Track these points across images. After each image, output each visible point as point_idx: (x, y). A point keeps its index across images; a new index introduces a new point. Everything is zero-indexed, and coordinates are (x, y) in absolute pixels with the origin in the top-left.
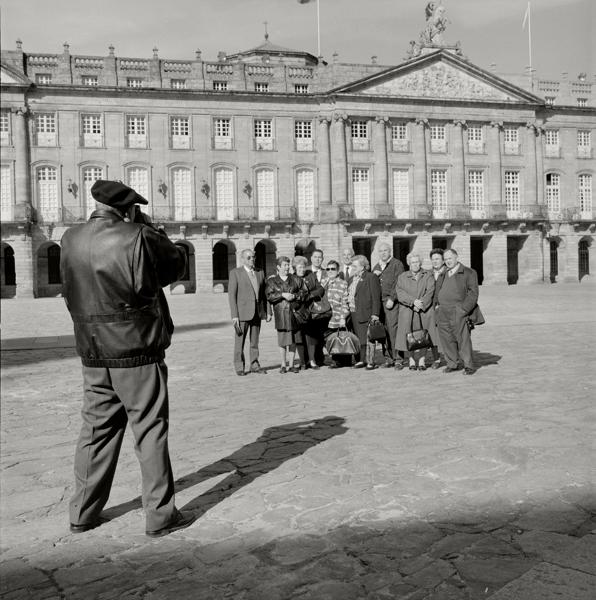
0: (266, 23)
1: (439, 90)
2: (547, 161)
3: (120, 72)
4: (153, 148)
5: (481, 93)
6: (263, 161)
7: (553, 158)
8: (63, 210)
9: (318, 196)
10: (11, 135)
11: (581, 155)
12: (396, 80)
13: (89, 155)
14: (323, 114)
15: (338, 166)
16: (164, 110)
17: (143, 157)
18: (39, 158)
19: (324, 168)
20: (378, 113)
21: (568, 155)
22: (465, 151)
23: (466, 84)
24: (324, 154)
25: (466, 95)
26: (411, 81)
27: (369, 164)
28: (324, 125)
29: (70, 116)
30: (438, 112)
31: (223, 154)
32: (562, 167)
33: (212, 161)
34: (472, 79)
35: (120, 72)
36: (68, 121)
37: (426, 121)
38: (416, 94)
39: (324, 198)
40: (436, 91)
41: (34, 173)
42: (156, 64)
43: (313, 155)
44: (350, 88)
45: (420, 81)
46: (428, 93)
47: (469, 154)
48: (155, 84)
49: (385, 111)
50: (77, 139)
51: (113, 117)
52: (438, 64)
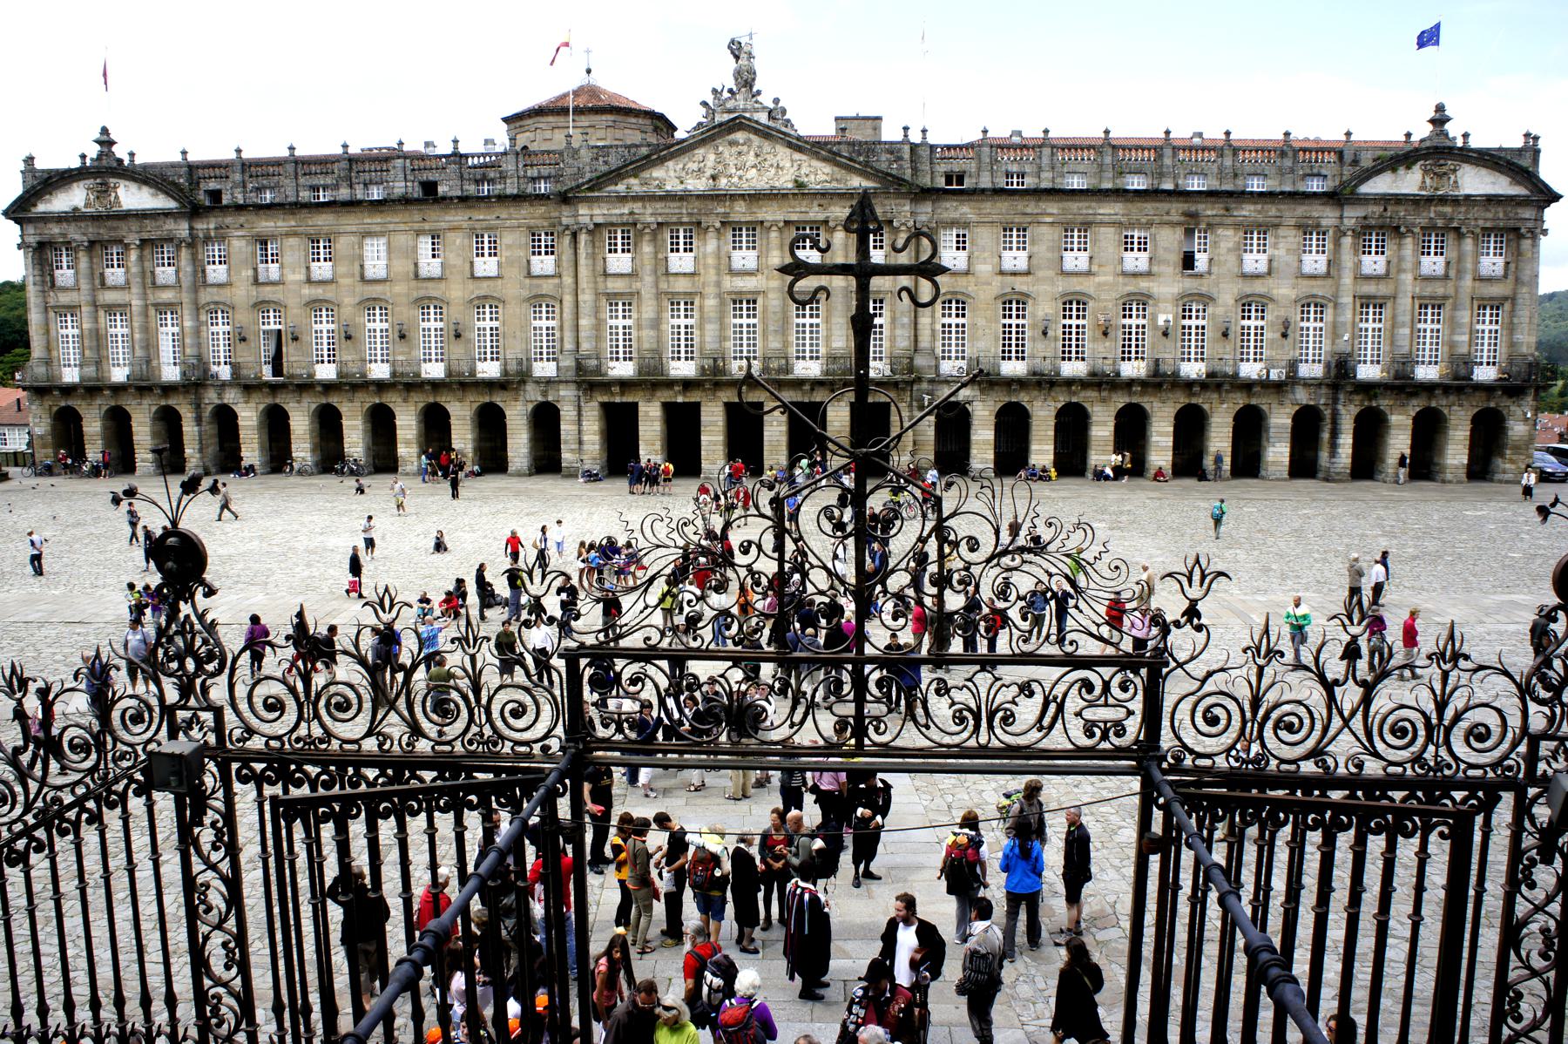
0: (588, 52)
1: (740, 178)
3: (302, 180)
4: (342, 281)
5: (812, 177)
6: (482, 293)
8: (236, 368)
10: (177, 272)
11: (1008, 265)
12: (670, 164)
13: (268, 293)
14: (565, 221)
16: (354, 229)
18: (208, 299)
19: (568, 299)
20: (642, 218)
21: (984, 268)
23: (788, 165)
24: (568, 280)
25: (785, 181)
26: (695, 166)
27: (631, 294)
28: (567, 240)
29: (243, 243)
30: (740, 211)
31: (430, 285)
32: (971, 289)
33: (415, 295)
34: (797, 156)
35: (302, 180)
36: (239, 245)
37: (718, 225)
38: (698, 185)
40: (735, 180)
42: (344, 164)
43: (556, 281)
44: (597, 183)
46: (723, 182)
48: (344, 193)
49: (648, 214)
50: (250, 273)
51: (292, 241)
52: (740, 136)
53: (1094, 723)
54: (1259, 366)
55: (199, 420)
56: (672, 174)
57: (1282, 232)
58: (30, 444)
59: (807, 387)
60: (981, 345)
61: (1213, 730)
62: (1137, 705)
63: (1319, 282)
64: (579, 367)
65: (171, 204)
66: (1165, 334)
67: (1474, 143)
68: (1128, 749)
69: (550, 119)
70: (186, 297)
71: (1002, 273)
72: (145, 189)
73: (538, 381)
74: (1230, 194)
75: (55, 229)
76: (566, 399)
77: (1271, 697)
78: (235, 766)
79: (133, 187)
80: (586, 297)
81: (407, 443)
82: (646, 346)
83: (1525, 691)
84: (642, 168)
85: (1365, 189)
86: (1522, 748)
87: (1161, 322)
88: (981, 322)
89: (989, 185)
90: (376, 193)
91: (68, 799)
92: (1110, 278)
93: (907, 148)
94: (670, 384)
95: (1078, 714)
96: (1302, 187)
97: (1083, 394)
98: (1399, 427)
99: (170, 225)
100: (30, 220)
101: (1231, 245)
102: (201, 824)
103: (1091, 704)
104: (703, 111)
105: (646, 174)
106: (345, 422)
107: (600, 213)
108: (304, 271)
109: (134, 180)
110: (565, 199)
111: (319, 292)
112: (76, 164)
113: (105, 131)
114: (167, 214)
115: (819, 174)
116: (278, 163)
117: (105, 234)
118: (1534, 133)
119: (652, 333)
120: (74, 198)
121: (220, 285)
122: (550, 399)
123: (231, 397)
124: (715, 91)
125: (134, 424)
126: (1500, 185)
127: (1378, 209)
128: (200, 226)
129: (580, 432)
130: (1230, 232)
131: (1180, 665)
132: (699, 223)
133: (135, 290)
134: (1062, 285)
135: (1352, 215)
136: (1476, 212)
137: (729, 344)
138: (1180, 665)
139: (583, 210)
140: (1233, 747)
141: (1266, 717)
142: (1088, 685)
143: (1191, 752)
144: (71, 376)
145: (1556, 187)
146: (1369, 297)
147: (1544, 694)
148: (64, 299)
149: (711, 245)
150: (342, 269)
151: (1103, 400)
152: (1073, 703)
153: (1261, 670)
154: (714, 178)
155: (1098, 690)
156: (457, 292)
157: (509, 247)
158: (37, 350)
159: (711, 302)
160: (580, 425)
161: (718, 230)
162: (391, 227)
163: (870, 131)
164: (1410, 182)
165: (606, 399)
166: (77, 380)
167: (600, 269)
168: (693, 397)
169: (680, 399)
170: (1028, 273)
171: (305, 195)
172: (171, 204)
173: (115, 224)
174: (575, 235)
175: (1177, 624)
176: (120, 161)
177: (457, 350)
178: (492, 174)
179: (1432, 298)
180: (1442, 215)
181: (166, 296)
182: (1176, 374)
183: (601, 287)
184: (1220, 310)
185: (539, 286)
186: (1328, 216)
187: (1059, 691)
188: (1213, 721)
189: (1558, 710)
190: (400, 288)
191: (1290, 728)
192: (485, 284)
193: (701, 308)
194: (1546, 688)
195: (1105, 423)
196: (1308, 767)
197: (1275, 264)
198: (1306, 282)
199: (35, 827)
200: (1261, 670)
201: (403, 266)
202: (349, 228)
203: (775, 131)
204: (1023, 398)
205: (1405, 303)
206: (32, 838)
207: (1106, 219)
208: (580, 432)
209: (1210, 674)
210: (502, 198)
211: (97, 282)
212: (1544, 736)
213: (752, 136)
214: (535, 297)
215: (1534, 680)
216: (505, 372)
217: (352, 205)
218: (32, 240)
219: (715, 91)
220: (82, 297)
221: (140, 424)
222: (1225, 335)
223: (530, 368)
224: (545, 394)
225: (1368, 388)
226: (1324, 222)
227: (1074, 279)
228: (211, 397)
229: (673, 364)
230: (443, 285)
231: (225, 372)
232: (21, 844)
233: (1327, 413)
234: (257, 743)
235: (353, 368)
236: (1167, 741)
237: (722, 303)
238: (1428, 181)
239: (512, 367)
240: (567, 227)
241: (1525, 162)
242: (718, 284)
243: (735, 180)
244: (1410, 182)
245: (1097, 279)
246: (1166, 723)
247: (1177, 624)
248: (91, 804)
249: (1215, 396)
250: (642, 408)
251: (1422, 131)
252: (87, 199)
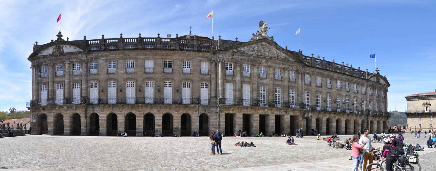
2: (306, 86)
7: (308, 85)
9: (210, 94)
12: (246, 47)
19: (213, 82)
24: (213, 76)
28: (213, 65)
39: (213, 95)
43: (209, 76)
60: (313, 103)
71: (317, 86)
73: (204, 106)
84: (238, 47)
88: (313, 98)
105: (239, 49)
122: (206, 113)
129: (219, 122)
134: (327, 91)
151: (335, 117)
157: (194, 66)
160: (219, 120)
165: (227, 112)
170: (321, 87)
174: (216, 64)
183: (225, 79)
195: (335, 122)
203: (272, 42)
208: (219, 122)
224: (205, 110)
240: (214, 61)
243: (263, 54)
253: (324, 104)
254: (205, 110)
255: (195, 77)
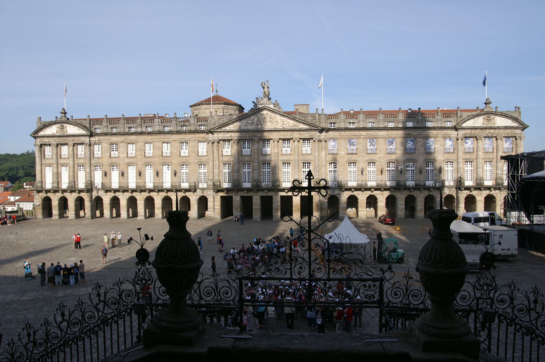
3: (126, 125)
5: (287, 125)
6: (183, 161)
12: (243, 121)
13: (114, 160)
14: (210, 139)
15: (216, 163)
16: (142, 140)
17: (134, 160)
19: (211, 163)
22: (280, 153)
24: (211, 157)
25: (279, 127)
28: (210, 144)
31: (166, 158)
34: (283, 118)
36: (105, 145)
41: (92, 168)
45: (255, 121)
47: (282, 154)
48: (139, 130)
50: (109, 154)
51: (123, 144)
53: (367, 295)
54: (432, 182)
55: (91, 201)
56: (243, 124)
57: (438, 139)
58: (34, 208)
59: (286, 191)
61: (396, 297)
62: (377, 290)
63: (451, 155)
64: (214, 185)
65: (83, 132)
66: (401, 172)
67: (499, 110)
68: (375, 301)
69: (205, 106)
70: (88, 162)
72: (76, 128)
74: (421, 128)
75: (46, 140)
76: (210, 195)
77: (411, 288)
78: (154, 308)
79: (72, 126)
80: (216, 163)
81: (158, 209)
82: (235, 178)
83: (474, 287)
85: (464, 125)
86: (475, 301)
87: (400, 168)
89: (344, 127)
90: (149, 130)
91: (109, 316)
92: (383, 155)
93: (317, 115)
94: (243, 190)
95: (363, 293)
96: (444, 125)
97: (375, 192)
98: (480, 201)
99: (83, 139)
100: (38, 137)
101: (421, 144)
102: (144, 323)
103: (366, 290)
104: (253, 104)
106: (138, 202)
107: (221, 136)
108: (126, 154)
109: (72, 124)
110: (211, 132)
111: (131, 160)
112: (54, 119)
113: (64, 109)
114: (82, 135)
115: (290, 123)
116: (119, 119)
117: (62, 140)
118: (518, 106)
119: (237, 174)
120: (53, 130)
121: (98, 158)
123: (101, 194)
124: (257, 98)
125: (69, 202)
126: (509, 123)
127: (469, 131)
128: (93, 139)
130: (421, 140)
131: (387, 281)
132: (252, 139)
133: (71, 159)
134: (368, 157)
135: (461, 133)
136: (502, 131)
137: (262, 177)
138: (387, 281)
139: (215, 135)
140: (402, 301)
141: (410, 294)
142: (365, 286)
143: (391, 302)
144: (48, 186)
145: (527, 123)
146: (467, 159)
147: (480, 288)
148: (48, 162)
149: (256, 146)
150: (138, 153)
151: (382, 194)
152: (362, 291)
153: (408, 282)
154: (257, 125)
155: (368, 287)
156: (175, 161)
157: (192, 147)
158: (38, 178)
159: (256, 164)
161: (258, 142)
162: (154, 140)
163: (306, 109)
164: (479, 122)
166: (51, 188)
167: (220, 154)
168: (250, 194)
169: (246, 195)
171: (127, 130)
172: (83, 132)
173: (66, 138)
175: (386, 271)
176: (68, 119)
177: (176, 179)
178: (186, 124)
179: (488, 159)
180: (491, 133)
181: (81, 161)
182: (405, 185)
184: (418, 165)
185: (201, 159)
186: (453, 133)
187: (358, 287)
188: (396, 295)
189: (483, 292)
190: (156, 160)
191: (415, 296)
192: (184, 158)
193: (253, 166)
194: (480, 286)
195: (382, 201)
196: (421, 306)
197: (436, 149)
198: (446, 155)
199: (100, 324)
200: (408, 282)
201: (158, 153)
202: (141, 140)
204: (356, 193)
205: (480, 161)
206: (99, 327)
207: (381, 136)
209: (395, 283)
210: (190, 132)
211: (59, 157)
212: (480, 298)
213: (269, 112)
214: (200, 162)
215: (477, 284)
216: (190, 186)
217: (142, 133)
218: (39, 143)
219: (257, 98)
220: (54, 161)
221: (71, 202)
222: (421, 172)
223: (198, 185)
224: (203, 193)
225: (468, 188)
226: (452, 136)
227: (371, 156)
228: (95, 194)
229: (244, 184)
230: (171, 158)
231: (100, 187)
232: (96, 328)
233: (455, 197)
234: (160, 302)
235: (141, 185)
236: (385, 300)
237: (259, 165)
238: (485, 122)
239: (193, 184)
241: (516, 115)
242: (258, 159)
244: (479, 122)
245: (379, 155)
246: (385, 295)
247: (386, 271)
248: (115, 318)
249: (418, 192)
250: (234, 198)
251: (482, 106)
252: (57, 131)
253: (361, 178)
254: (203, 193)
255: (193, 160)
